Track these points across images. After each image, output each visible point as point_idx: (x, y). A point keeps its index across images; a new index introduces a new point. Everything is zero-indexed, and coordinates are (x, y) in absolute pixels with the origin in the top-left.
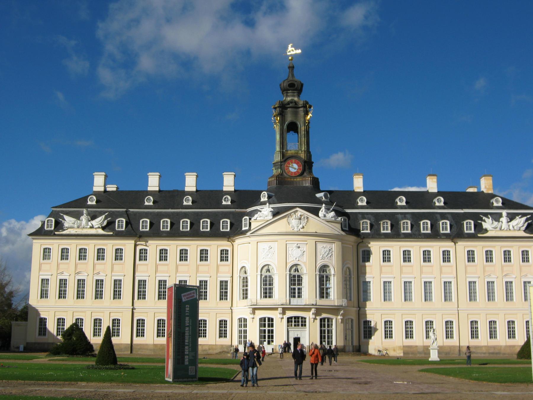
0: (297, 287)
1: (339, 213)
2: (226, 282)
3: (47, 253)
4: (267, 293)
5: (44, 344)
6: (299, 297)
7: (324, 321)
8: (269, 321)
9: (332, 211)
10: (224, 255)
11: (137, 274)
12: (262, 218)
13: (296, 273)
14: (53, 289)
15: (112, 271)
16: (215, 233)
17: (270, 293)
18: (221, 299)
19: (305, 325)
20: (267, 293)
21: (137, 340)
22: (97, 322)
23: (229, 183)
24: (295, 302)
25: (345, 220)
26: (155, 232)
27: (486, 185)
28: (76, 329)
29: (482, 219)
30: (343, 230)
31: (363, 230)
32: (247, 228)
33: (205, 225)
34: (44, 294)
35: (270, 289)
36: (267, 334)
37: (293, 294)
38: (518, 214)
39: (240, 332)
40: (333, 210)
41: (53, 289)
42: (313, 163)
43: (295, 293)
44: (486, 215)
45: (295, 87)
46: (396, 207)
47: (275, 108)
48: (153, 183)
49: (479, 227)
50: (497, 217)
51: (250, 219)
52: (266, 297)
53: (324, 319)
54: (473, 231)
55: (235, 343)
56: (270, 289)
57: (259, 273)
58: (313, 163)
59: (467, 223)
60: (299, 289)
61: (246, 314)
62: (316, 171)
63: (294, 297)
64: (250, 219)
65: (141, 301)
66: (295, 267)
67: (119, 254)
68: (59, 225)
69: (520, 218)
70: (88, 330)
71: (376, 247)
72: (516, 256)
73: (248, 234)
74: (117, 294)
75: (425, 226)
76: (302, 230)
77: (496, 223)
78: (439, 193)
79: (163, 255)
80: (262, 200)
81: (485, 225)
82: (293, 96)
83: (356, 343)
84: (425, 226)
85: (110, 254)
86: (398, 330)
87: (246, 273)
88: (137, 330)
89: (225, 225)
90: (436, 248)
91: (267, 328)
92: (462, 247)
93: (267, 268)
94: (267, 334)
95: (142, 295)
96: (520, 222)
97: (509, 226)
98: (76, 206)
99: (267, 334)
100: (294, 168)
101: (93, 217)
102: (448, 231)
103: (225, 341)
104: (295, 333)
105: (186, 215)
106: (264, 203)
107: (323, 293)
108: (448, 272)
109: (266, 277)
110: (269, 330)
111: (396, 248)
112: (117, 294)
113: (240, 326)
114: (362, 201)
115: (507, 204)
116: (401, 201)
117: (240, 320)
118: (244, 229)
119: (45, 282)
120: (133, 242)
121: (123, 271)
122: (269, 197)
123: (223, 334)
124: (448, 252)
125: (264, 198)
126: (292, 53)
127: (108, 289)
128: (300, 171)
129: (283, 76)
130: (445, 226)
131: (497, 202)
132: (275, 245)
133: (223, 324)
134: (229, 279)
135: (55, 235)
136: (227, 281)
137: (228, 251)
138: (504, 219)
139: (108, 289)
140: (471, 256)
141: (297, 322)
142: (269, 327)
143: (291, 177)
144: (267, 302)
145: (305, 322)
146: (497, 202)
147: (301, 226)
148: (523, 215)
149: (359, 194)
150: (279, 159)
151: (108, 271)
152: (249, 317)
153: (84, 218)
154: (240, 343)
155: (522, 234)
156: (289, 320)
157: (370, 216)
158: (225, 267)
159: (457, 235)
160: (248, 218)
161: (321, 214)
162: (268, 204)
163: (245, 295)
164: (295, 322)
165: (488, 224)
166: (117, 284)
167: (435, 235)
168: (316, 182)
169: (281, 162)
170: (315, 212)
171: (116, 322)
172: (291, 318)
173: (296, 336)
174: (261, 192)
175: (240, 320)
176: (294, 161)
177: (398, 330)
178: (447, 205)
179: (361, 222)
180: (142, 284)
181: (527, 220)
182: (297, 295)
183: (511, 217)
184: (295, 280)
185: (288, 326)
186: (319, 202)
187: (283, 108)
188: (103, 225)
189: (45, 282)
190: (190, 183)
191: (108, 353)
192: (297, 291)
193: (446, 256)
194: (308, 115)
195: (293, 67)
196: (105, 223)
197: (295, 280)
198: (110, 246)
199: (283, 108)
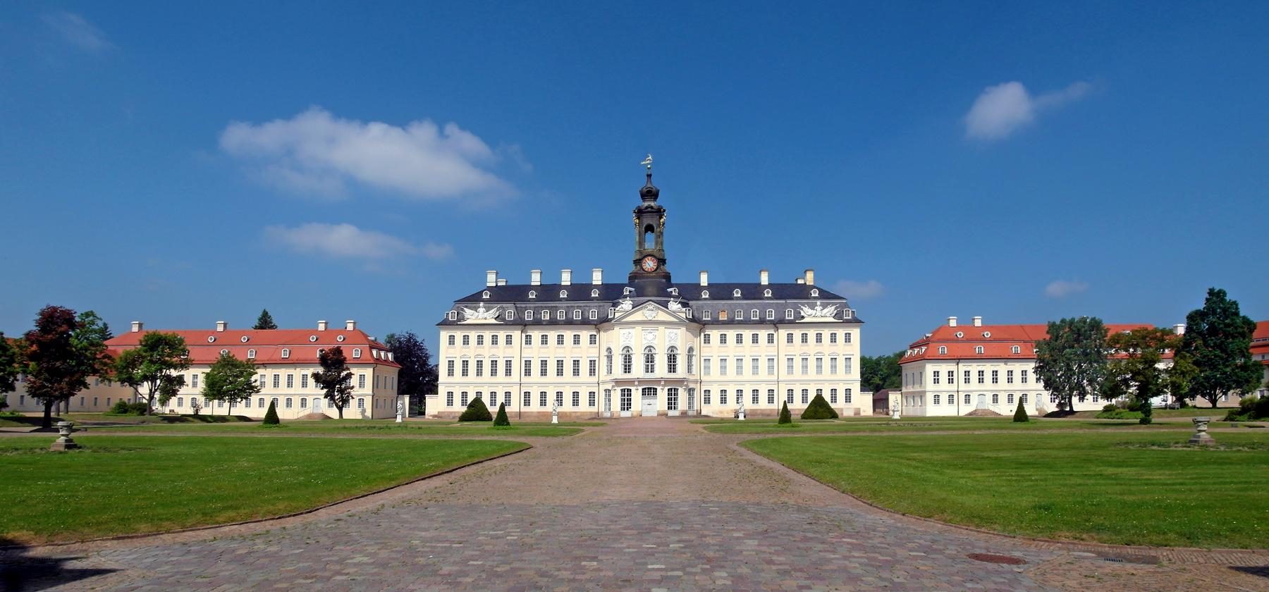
3: (452, 340)
4: (627, 369)
14: (458, 368)
20: (627, 369)
21: (524, 409)
22: (493, 395)
23: (597, 278)
27: (810, 279)
28: (478, 401)
34: (451, 373)
41: (458, 368)
45: (650, 194)
48: (536, 279)
55: (602, 409)
62: (667, 268)
66: (650, 348)
67: (509, 340)
68: (461, 317)
70: (486, 400)
74: (508, 372)
77: (810, 312)
78: (770, 286)
86: (731, 396)
95: (528, 372)
96: (831, 310)
98: (473, 300)
100: (650, 264)
103: (594, 409)
112: (508, 372)
114: (705, 295)
116: (737, 293)
119: (451, 363)
123: (592, 403)
127: (501, 368)
131: (815, 293)
133: (592, 394)
138: (819, 308)
139: (501, 368)
140: (790, 338)
141: (649, 392)
146: (815, 293)
148: (833, 304)
149: (704, 288)
151: (502, 352)
153: (481, 310)
155: (832, 320)
165: (806, 311)
166: (508, 363)
168: (667, 277)
170: (665, 305)
171: (508, 394)
174: (623, 286)
177: (731, 396)
178: (775, 297)
180: (528, 363)
183: (824, 306)
184: (650, 359)
186: (669, 295)
187: (640, 212)
189: (451, 363)
190: (566, 279)
191: (502, 418)
193: (771, 339)
197: (650, 359)
199: (640, 212)
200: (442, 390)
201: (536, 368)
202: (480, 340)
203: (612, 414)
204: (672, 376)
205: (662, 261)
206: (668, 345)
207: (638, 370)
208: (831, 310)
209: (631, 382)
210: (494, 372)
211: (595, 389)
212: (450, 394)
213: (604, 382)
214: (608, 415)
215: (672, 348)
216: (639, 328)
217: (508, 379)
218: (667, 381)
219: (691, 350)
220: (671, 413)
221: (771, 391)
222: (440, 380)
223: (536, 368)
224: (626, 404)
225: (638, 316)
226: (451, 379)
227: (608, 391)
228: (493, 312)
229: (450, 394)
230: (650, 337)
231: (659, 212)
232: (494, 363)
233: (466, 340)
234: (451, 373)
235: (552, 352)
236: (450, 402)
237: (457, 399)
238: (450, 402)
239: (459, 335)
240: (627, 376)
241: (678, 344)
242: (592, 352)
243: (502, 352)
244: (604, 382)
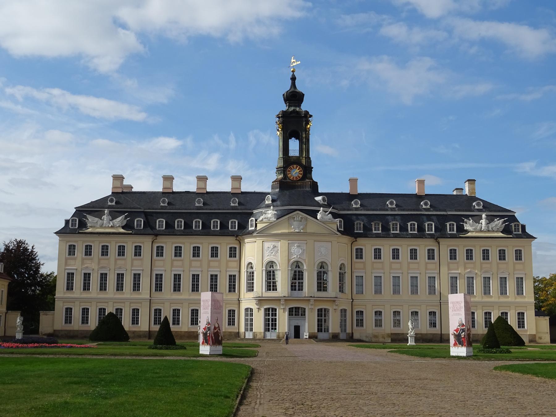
0: (297, 281)
1: (335, 216)
4: (271, 285)
5: (70, 331)
6: (299, 290)
7: (322, 312)
8: (272, 311)
9: (329, 214)
10: (233, 253)
11: (154, 268)
12: (266, 220)
13: (297, 269)
14: (78, 281)
15: (132, 266)
16: (224, 231)
18: (230, 291)
19: (305, 315)
20: (271, 285)
24: (296, 293)
25: (340, 222)
26: (170, 230)
29: (463, 221)
30: (338, 231)
31: (357, 230)
32: (253, 228)
33: (215, 224)
34: (70, 287)
36: (270, 323)
37: (293, 288)
38: (497, 216)
39: (246, 320)
40: (330, 213)
41: (78, 281)
42: (312, 168)
43: (295, 286)
44: (467, 217)
46: (387, 210)
47: (279, 117)
49: (461, 229)
50: (477, 219)
51: (256, 220)
52: (270, 290)
53: (321, 309)
54: (455, 232)
56: (274, 283)
57: (264, 269)
58: (312, 168)
59: (450, 225)
60: (299, 283)
61: (253, 305)
62: (315, 176)
63: (295, 290)
64: (256, 220)
65: (158, 293)
66: (297, 264)
67: (138, 251)
68: (83, 225)
69: (498, 220)
71: (368, 246)
72: (494, 255)
73: (255, 234)
74: (136, 287)
75: (412, 226)
79: (178, 252)
80: (267, 202)
81: (467, 227)
82: (296, 106)
83: (349, 330)
84: (412, 226)
85: (130, 251)
87: (252, 268)
88: (155, 318)
89: (233, 224)
90: (423, 246)
91: (270, 317)
92: (446, 245)
93: (271, 264)
94: (270, 323)
95: (159, 288)
96: (498, 223)
97: (488, 227)
99: (270, 323)
100: (295, 172)
101: (114, 218)
102: (433, 232)
104: (297, 321)
105: (198, 215)
106: (268, 206)
107: (322, 286)
108: (432, 268)
110: (272, 319)
111: (387, 246)
112: (136, 287)
113: (246, 315)
115: (488, 206)
117: (247, 310)
118: (250, 229)
120: (151, 240)
121: (143, 266)
122: (273, 201)
124: (433, 250)
125: (268, 202)
126: (294, 64)
127: (128, 281)
128: (301, 176)
129: (287, 87)
130: (430, 227)
132: (279, 244)
134: (237, 274)
135: (79, 233)
136: (235, 275)
137: (236, 248)
138: (483, 221)
139: (128, 281)
140: (453, 255)
142: (272, 316)
143: (293, 181)
144: (272, 294)
145: (305, 312)
147: (302, 227)
148: (501, 217)
150: (282, 164)
151: (129, 265)
152: (254, 306)
154: (246, 330)
155: (501, 234)
156: (291, 310)
157: (363, 217)
158: (233, 263)
159: (441, 234)
160: (254, 219)
161: (319, 216)
162: (272, 207)
163: (250, 288)
164: (295, 312)
166: (137, 277)
167: (421, 234)
168: (315, 185)
169: (283, 167)
172: (292, 308)
173: (296, 324)
175: (247, 310)
176: (295, 166)
179: (356, 223)
180: (159, 277)
181: (505, 222)
182: (297, 288)
185: (289, 315)
186: (318, 205)
188: (124, 225)
192: (297, 284)
193: (431, 255)
194: (309, 124)
195: (295, 78)
196: (125, 222)
198: (130, 244)
200: (60, 307)
201: (168, 283)
202: (105, 251)
203: (255, 335)
204: (322, 294)
205: (307, 169)
206: (318, 261)
208: (498, 223)
209: (277, 300)
210: (120, 287)
212: (69, 311)
214: (249, 335)
215: (322, 265)
217: (135, 296)
218: (318, 300)
219: (342, 267)
220: (322, 335)
221: (432, 314)
222: (57, 295)
223: (168, 283)
226: (69, 295)
227: (249, 311)
228: (120, 220)
231: (307, 116)
232: (120, 277)
233: (88, 251)
234: (70, 287)
235: (186, 266)
240: (272, 294)
241: (328, 260)
243: (129, 265)
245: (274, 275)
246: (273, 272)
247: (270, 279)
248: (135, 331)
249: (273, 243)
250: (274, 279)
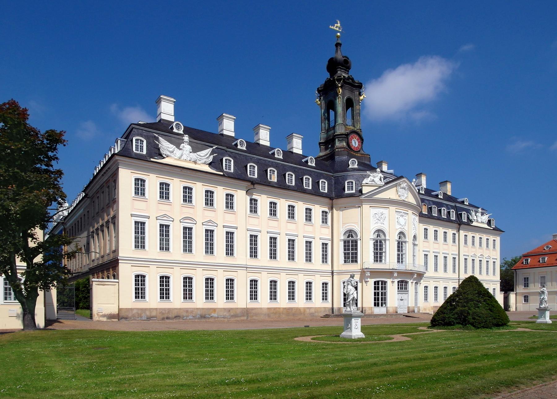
2: (326, 244)
4: (378, 256)
12: (373, 183)
17: (381, 257)
20: (378, 256)
32: (354, 191)
35: (381, 254)
52: (377, 261)
76: (406, 200)
93: (379, 232)
109: (377, 241)
151: (220, 218)
200: (127, 272)
207: (390, 260)
211: (328, 280)
212: (140, 280)
213: (340, 273)
216: (393, 209)
224: (380, 298)
225: (391, 194)
229: (140, 280)
230: (402, 220)
235: (283, 227)
236: (140, 293)
237: (152, 287)
238: (140, 293)
239: (153, 182)
242: (326, 233)
243: (220, 218)
244: (340, 273)
245: (381, 246)
246: (381, 242)
247: (377, 249)
248: (232, 309)
249: (381, 210)
250: (381, 249)
